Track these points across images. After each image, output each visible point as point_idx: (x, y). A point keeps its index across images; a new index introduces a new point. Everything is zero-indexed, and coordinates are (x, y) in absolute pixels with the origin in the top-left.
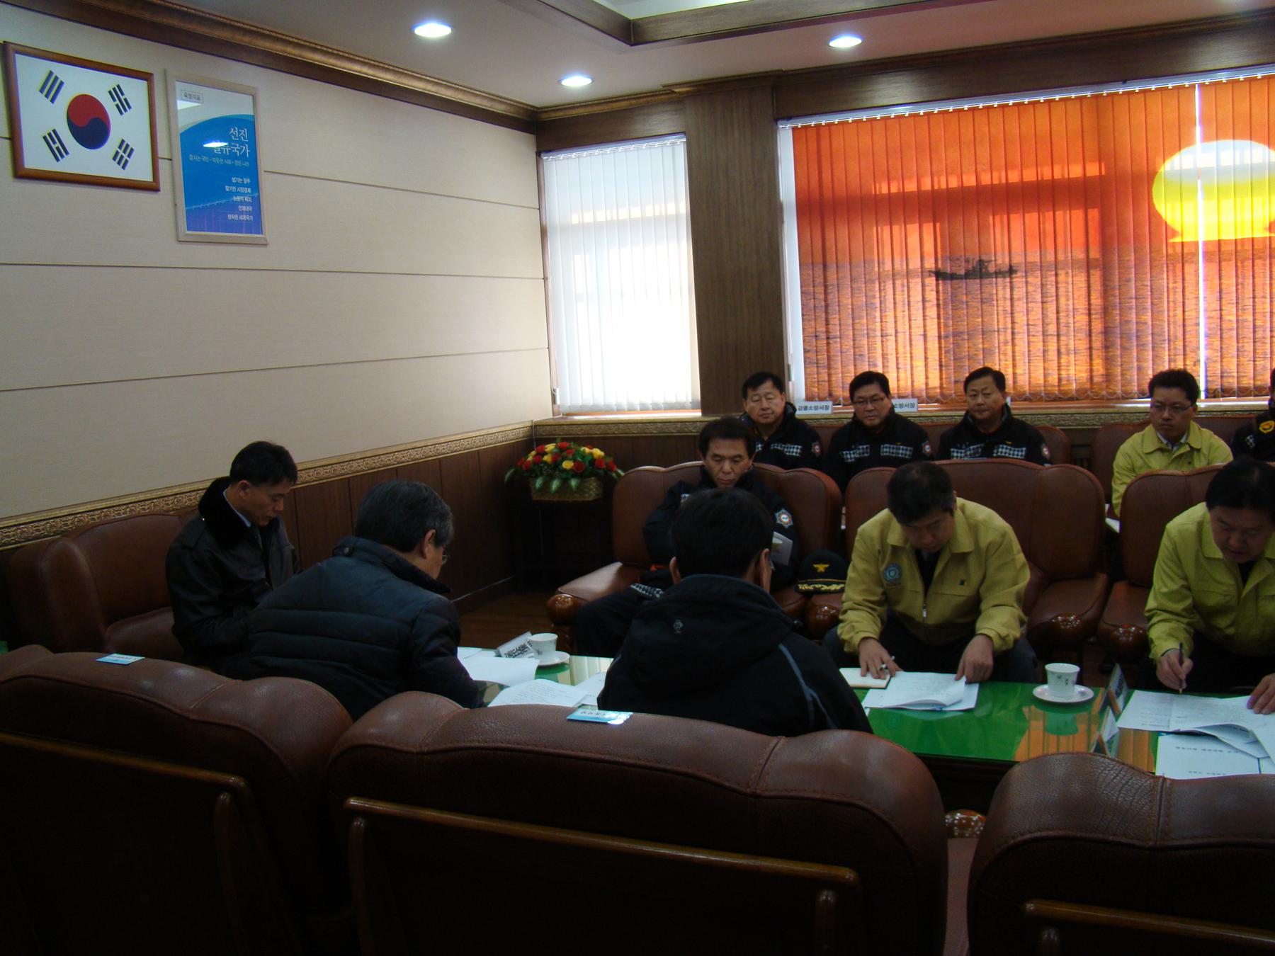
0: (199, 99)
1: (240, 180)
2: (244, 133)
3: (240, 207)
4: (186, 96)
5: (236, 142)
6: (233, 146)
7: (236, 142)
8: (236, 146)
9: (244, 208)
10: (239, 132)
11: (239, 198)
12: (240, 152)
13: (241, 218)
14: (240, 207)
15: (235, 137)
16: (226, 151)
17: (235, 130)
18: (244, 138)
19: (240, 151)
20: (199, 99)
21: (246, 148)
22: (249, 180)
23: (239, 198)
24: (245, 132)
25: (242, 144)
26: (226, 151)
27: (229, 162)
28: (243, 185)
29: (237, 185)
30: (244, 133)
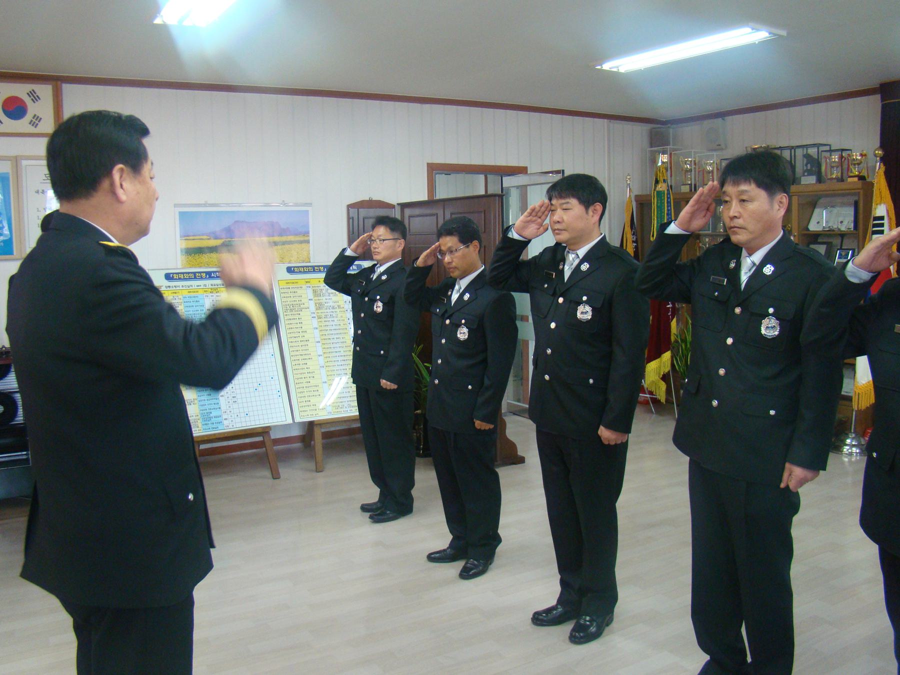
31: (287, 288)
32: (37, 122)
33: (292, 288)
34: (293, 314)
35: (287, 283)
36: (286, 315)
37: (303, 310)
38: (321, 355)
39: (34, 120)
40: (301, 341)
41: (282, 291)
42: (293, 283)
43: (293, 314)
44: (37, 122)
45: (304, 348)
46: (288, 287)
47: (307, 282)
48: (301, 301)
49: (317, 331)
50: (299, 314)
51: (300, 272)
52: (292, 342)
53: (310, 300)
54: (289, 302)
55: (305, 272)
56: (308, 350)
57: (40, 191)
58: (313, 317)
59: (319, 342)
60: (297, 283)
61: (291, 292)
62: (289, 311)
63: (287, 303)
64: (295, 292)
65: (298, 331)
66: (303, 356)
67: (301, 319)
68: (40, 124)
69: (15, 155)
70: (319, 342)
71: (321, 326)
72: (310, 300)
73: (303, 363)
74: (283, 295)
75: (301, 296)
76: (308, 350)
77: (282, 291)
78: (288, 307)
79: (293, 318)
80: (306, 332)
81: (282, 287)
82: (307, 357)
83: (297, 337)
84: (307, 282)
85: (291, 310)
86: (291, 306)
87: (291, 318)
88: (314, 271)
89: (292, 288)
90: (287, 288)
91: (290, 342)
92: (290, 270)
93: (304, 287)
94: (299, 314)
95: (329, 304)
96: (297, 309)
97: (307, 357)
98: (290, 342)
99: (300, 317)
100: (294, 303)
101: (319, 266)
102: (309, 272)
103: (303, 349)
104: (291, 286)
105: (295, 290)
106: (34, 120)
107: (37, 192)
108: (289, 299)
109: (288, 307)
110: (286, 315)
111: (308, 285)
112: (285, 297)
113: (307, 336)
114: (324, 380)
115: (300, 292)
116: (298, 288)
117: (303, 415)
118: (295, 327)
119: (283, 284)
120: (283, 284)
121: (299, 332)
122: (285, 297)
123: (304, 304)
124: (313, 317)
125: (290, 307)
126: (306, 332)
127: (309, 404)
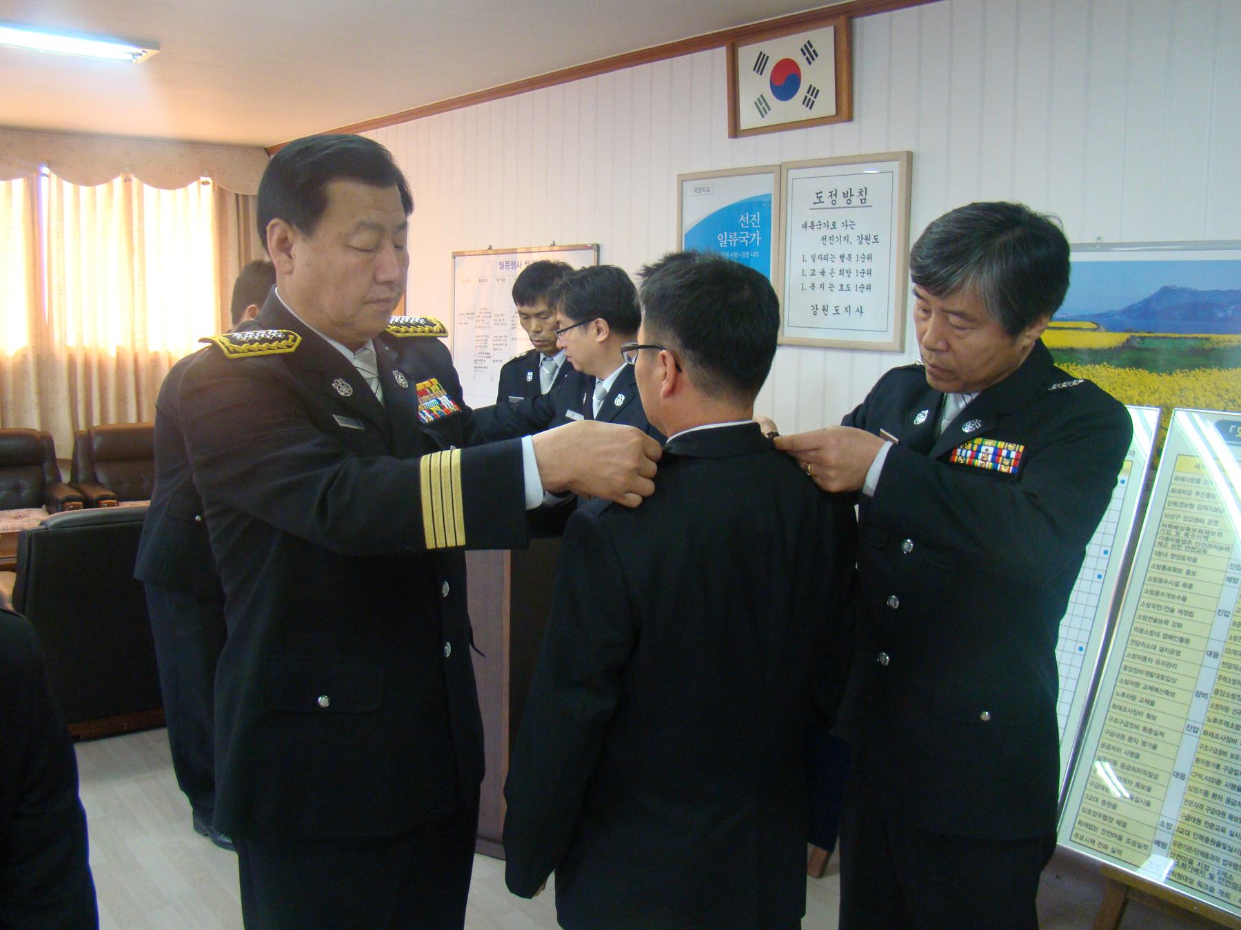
2: (756, 218)
5: (746, 230)
7: (746, 230)
8: (744, 235)
15: (745, 225)
17: (745, 216)
18: (756, 224)
19: (749, 240)
21: (757, 236)
24: (757, 217)
30: (756, 218)
34: (1179, 557)
37: (1211, 551)
38: (1205, 695)
40: (1166, 636)
43: (1179, 557)
45: (1166, 657)
49: (1224, 622)
50: (1195, 560)
52: (1141, 631)
56: (1175, 666)
58: (1229, 579)
59: (1216, 655)
62: (1170, 543)
63: (1175, 522)
65: (1171, 606)
66: (1155, 679)
67: (1194, 574)
70: (1216, 655)
73: (1146, 697)
76: (1175, 666)
78: (1173, 532)
79: (1173, 565)
80: (1191, 614)
82: (1163, 685)
83: (1161, 622)
86: (1182, 534)
87: (1168, 565)
91: (1136, 629)
97: (1163, 685)
98: (1136, 629)
99: (1191, 569)
100: (1192, 525)
103: (1162, 659)
110: (1160, 554)
113: (1188, 627)
114: (1180, 769)
117: (1081, 833)
118: (1166, 591)
121: (1172, 611)
124: (1229, 579)
125: (1177, 534)
126: (1191, 614)
127: (1109, 815)
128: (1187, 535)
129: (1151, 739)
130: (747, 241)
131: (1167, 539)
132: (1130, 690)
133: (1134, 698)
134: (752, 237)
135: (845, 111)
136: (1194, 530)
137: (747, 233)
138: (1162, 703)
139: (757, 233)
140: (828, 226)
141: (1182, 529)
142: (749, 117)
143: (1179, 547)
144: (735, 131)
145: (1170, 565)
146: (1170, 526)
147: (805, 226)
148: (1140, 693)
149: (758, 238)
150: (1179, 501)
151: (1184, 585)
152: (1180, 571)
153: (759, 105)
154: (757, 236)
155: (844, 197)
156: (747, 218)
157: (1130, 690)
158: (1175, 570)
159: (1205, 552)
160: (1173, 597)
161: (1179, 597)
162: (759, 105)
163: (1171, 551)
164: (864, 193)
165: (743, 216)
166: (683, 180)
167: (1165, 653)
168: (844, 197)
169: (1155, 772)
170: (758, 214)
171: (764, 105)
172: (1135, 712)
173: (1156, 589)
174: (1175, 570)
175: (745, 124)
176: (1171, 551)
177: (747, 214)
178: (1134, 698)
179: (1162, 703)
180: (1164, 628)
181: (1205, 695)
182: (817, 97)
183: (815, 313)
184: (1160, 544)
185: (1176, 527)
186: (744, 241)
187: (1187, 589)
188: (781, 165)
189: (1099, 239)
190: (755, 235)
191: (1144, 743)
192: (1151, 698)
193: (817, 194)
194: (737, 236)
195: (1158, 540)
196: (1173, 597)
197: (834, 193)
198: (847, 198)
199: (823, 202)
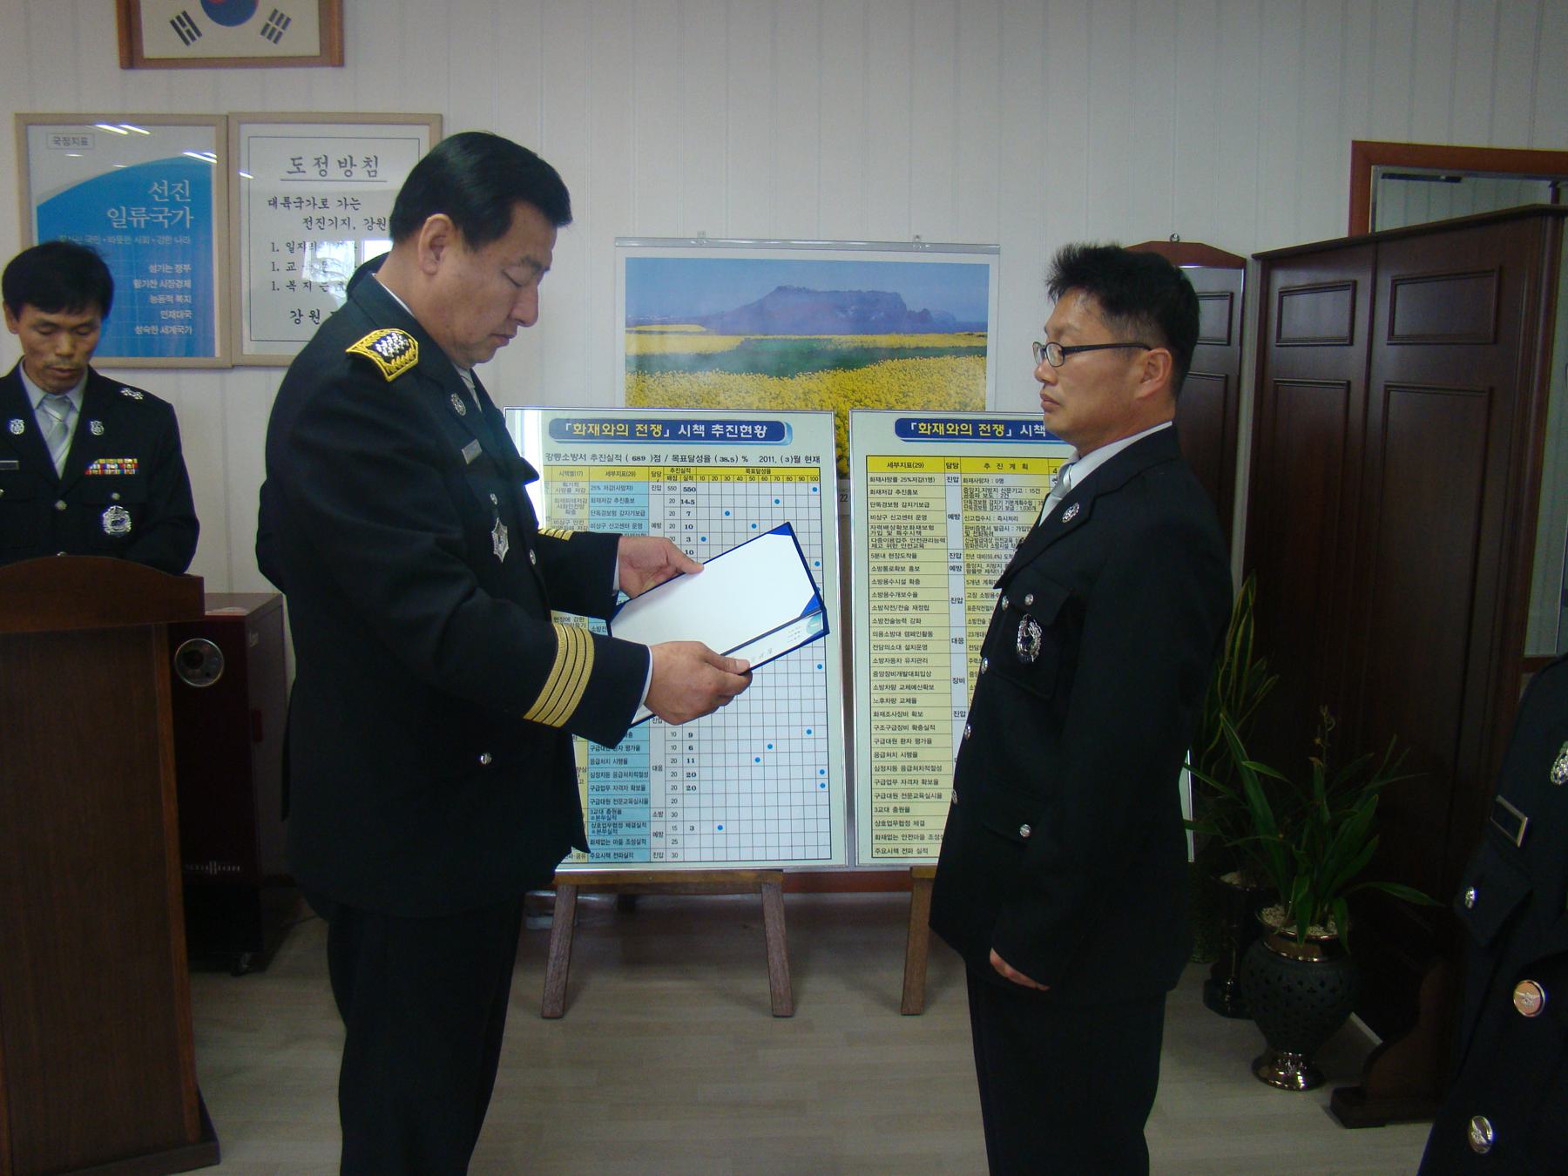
0: (84, 142)
1: (167, 268)
3: (163, 312)
4: (57, 142)
5: (163, 204)
6: (153, 212)
7: (163, 204)
8: (162, 212)
9: (173, 314)
10: (171, 188)
11: (161, 299)
12: (169, 222)
13: (165, 330)
14: (163, 312)
15: (161, 196)
16: (139, 222)
17: (162, 184)
18: (183, 196)
19: (170, 219)
20: (84, 142)
22: (187, 267)
23: (161, 299)
25: (174, 205)
26: (139, 222)
27: (145, 240)
28: (174, 276)
29: (161, 276)
30: (183, 188)
31: (889, 479)
32: (279, 28)
33: (904, 479)
34: (897, 556)
35: (891, 465)
36: (877, 556)
37: (927, 545)
38: (962, 681)
39: (273, 24)
40: (907, 634)
41: (875, 486)
42: (909, 466)
43: (897, 556)
44: (279, 28)
45: (913, 654)
46: (892, 476)
47: (949, 466)
48: (925, 517)
49: (959, 609)
50: (915, 556)
51: (935, 435)
52: (881, 634)
53: (951, 517)
54: (888, 520)
55: (948, 437)
56: (925, 660)
57: (281, 200)
58: (953, 568)
59: (961, 641)
60: (921, 465)
61: (898, 492)
62: (885, 544)
64: (909, 492)
65: (904, 604)
66: (909, 677)
67: (917, 569)
68: (286, 34)
69: (225, 112)
70: (961, 641)
71: (975, 595)
72: (951, 517)
73: (906, 697)
74: (874, 498)
75: (927, 505)
76: (925, 660)
77: (875, 486)
78: (885, 532)
79: (894, 565)
80: (927, 608)
81: (875, 476)
82: (919, 681)
83: (898, 621)
84: (949, 466)
85: (892, 544)
86: (894, 533)
87: (889, 565)
88: (976, 435)
89: (904, 479)
90: (889, 479)
91: (875, 634)
92: (904, 429)
93: (940, 479)
94: (915, 556)
95: (1005, 534)
96: (908, 542)
97: (919, 681)
98: (875, 634)
99: (914, 565)
100: (902, 522)
101: (992, 422)
102: (961, 437)
103: (911, 657)
104: (900, 473)
105: (912, 486)
106: (273, 24)
107: (274, 203)
108: (889, 512)
109: (885, 532)
110: (877, 556)
111: (953, 473)
112: (879, 504)
113: (927, 621)
115: (924, 492)
116: (921, 480)
118: (895, 591)
119: (880, 468)
120: (880, 468)
121: (907, 609)
122: (879, 504)
123: (931, 528)
124: (953, 568)
126: (927, 608)
128: (899, 533)
129: (923, 735)
130: (166, 221)
131: (880, 540)
132: (887, 694)
133: (893, 701)
134: (175, 215)
135: (332, 52)
136: (905, 528)
137: (166, 209)
138: (923, 698)
139: (185, 210)
140: (314, 204)
141: (893, 528)
142: (157, 39)
143: (895, 546)
144: (131, 55)
145: (892, 564)
146: (880, 527)
147: (274, 203)
148: (899, 695)
149: (188, 217)
150: (881, 501)
151: (911, 581)
152: (903, 569)
153: (180, 26)
154: (184, 216)
155: (341, 167)
156: (166, 188)
157: (887, 694)
158: (897, 569)
159: (922, 546)
160: (904, 595)
161: (909, 595)
162: (180, 26)
163: (887, 552)
164: (373, 164)
165: (156, 184)
166: (25, 122)
167: (911, 651)
168: (341, 167)
169: (936, 764)
170: (187, 182)
171: (189, 27)
172: (900, 714)
173: (883, 591)
174: (897, 569)
175: (150, 50)
176: (887, 552)
177: (166, 182)
178: (893, 701)
179: (923, 698)
180: (903, 627)
181: (962, 681)
182: (288, 28)
183: (298, 322)
184: (875, 546)
185: (887, 527)
186: (161, 219)
187: (915, 585)
188: (227, 117)
189: (918, 237)
190: (181, 212)
191: (918, 741)
192: (912, 697)
193: (293, 159)
194: (147, 213)
195: (871, 543)
196: (904, 595)
197: (323, 160)
198: (346, 169)
199: (304, 172)
